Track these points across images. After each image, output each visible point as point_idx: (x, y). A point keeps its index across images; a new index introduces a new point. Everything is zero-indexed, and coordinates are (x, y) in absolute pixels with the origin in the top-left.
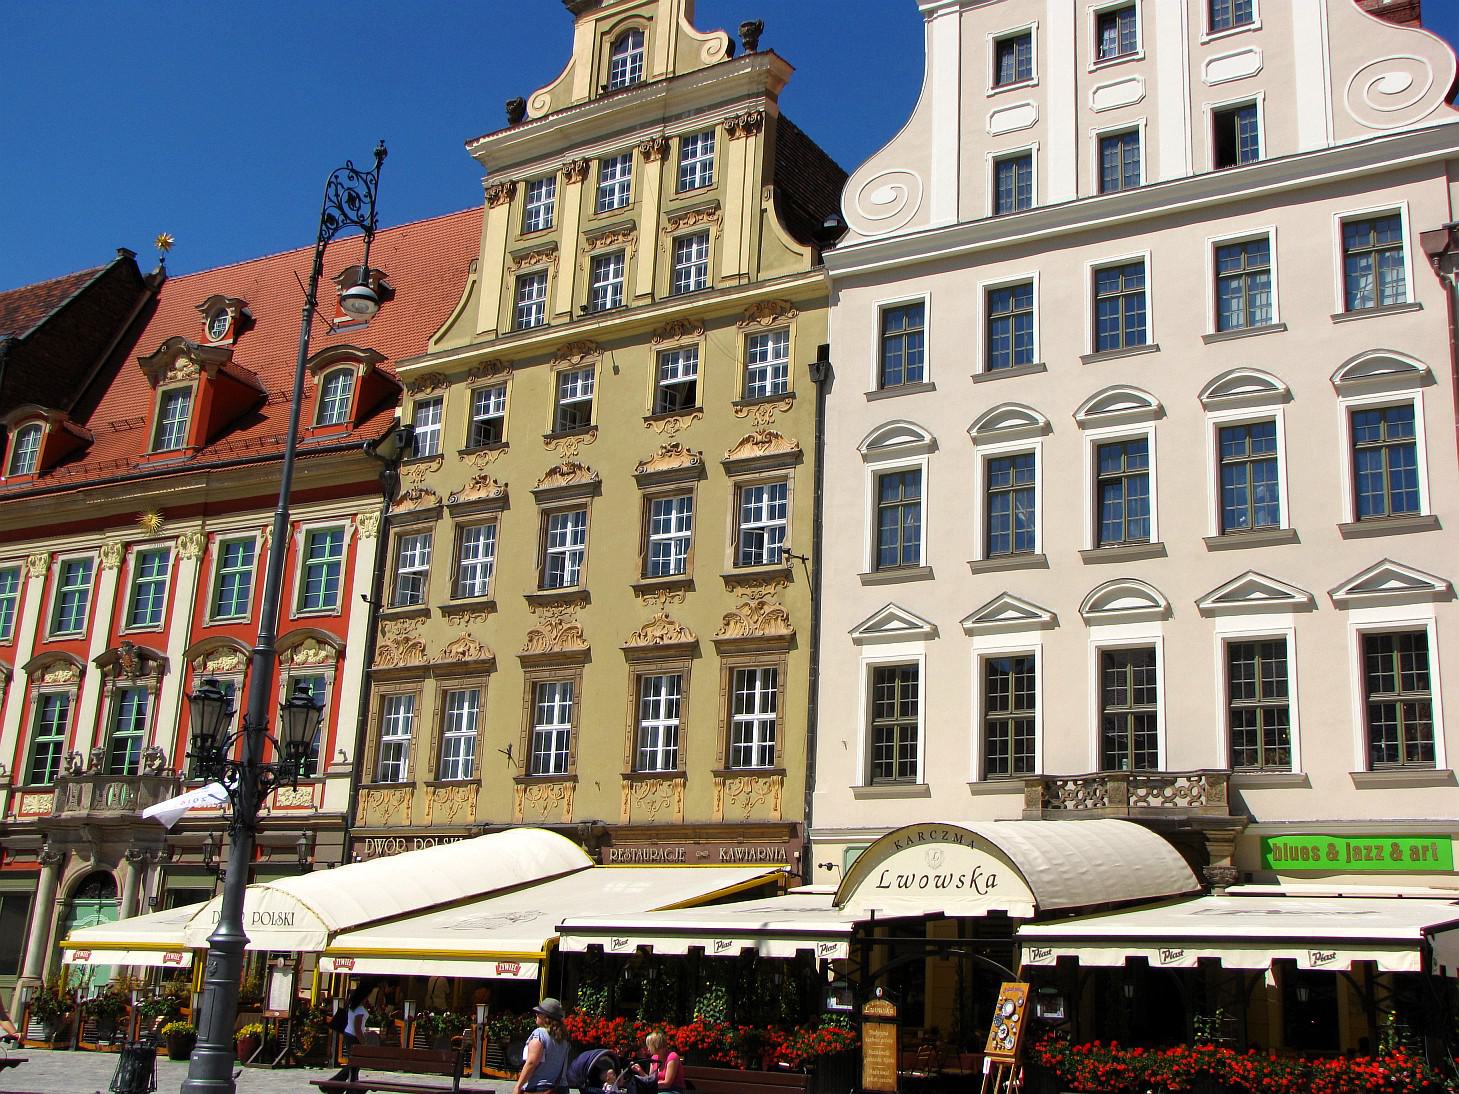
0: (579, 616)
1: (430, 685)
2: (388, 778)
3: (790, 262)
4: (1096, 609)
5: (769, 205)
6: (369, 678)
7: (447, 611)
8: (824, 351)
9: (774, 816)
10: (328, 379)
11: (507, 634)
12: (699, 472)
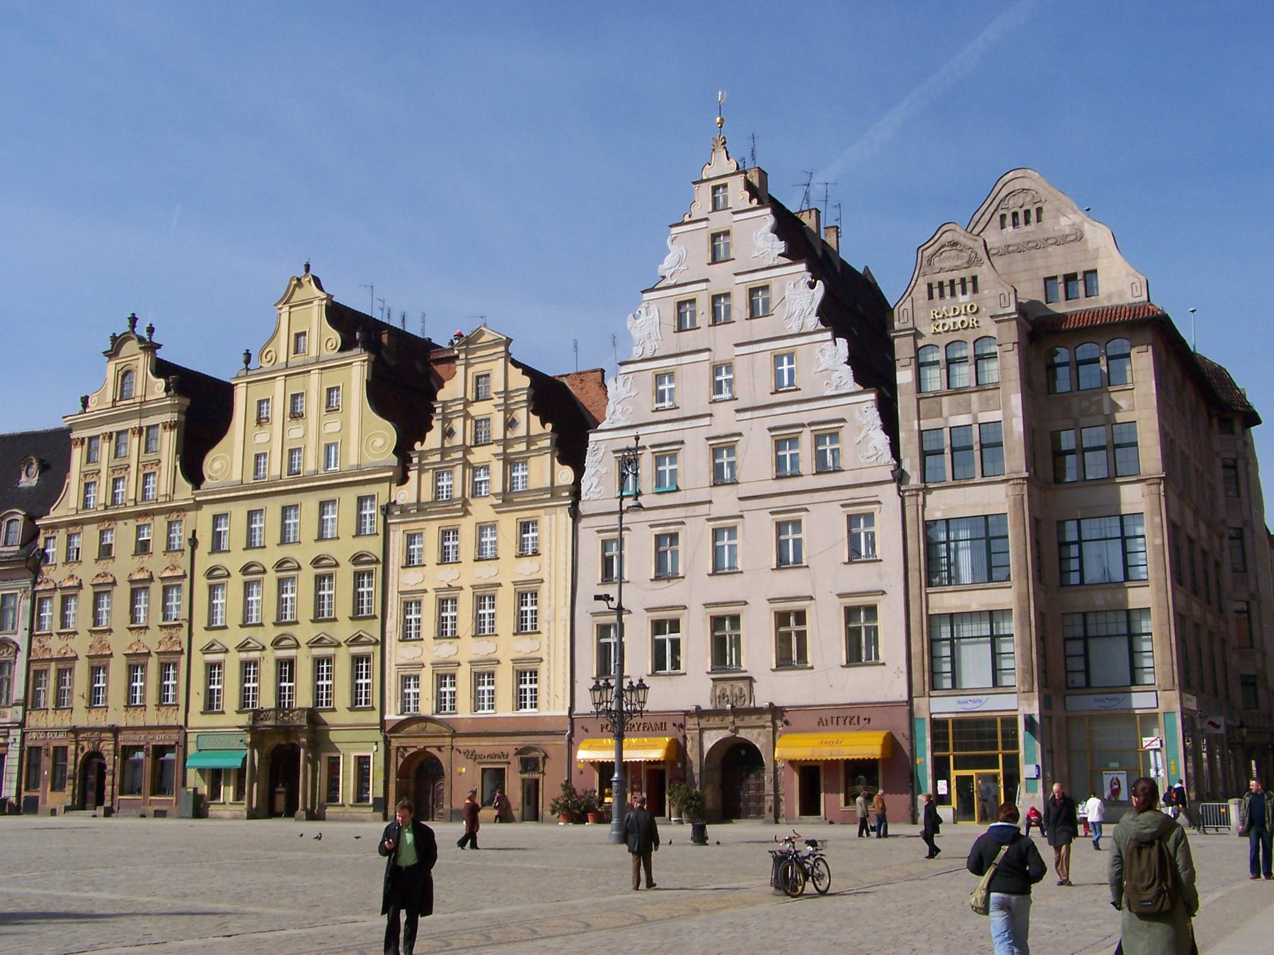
0: (108, 638)
1: (53, 665)
2: (36, 706)
3: (185, 491)
4: (276, 643)
5: (178, 464)
6: (29, 663)
7: (59, 634)
8: (194, 532)
9: (174, 723)
10: (9, 522)
11: (81, 645)
12: (151, 579)
